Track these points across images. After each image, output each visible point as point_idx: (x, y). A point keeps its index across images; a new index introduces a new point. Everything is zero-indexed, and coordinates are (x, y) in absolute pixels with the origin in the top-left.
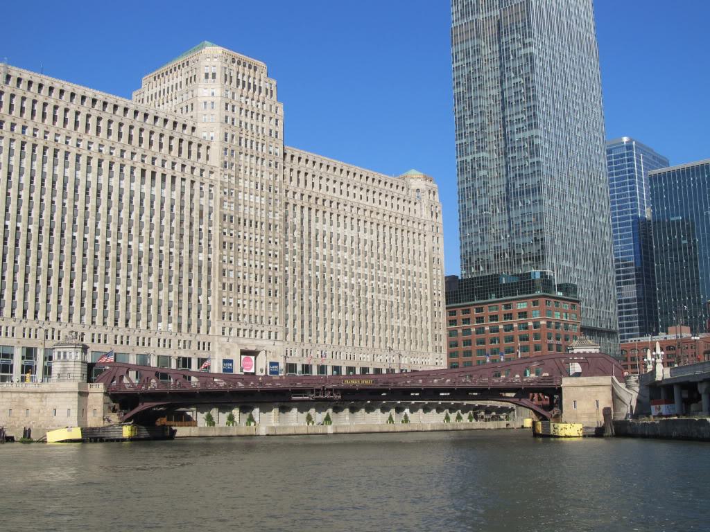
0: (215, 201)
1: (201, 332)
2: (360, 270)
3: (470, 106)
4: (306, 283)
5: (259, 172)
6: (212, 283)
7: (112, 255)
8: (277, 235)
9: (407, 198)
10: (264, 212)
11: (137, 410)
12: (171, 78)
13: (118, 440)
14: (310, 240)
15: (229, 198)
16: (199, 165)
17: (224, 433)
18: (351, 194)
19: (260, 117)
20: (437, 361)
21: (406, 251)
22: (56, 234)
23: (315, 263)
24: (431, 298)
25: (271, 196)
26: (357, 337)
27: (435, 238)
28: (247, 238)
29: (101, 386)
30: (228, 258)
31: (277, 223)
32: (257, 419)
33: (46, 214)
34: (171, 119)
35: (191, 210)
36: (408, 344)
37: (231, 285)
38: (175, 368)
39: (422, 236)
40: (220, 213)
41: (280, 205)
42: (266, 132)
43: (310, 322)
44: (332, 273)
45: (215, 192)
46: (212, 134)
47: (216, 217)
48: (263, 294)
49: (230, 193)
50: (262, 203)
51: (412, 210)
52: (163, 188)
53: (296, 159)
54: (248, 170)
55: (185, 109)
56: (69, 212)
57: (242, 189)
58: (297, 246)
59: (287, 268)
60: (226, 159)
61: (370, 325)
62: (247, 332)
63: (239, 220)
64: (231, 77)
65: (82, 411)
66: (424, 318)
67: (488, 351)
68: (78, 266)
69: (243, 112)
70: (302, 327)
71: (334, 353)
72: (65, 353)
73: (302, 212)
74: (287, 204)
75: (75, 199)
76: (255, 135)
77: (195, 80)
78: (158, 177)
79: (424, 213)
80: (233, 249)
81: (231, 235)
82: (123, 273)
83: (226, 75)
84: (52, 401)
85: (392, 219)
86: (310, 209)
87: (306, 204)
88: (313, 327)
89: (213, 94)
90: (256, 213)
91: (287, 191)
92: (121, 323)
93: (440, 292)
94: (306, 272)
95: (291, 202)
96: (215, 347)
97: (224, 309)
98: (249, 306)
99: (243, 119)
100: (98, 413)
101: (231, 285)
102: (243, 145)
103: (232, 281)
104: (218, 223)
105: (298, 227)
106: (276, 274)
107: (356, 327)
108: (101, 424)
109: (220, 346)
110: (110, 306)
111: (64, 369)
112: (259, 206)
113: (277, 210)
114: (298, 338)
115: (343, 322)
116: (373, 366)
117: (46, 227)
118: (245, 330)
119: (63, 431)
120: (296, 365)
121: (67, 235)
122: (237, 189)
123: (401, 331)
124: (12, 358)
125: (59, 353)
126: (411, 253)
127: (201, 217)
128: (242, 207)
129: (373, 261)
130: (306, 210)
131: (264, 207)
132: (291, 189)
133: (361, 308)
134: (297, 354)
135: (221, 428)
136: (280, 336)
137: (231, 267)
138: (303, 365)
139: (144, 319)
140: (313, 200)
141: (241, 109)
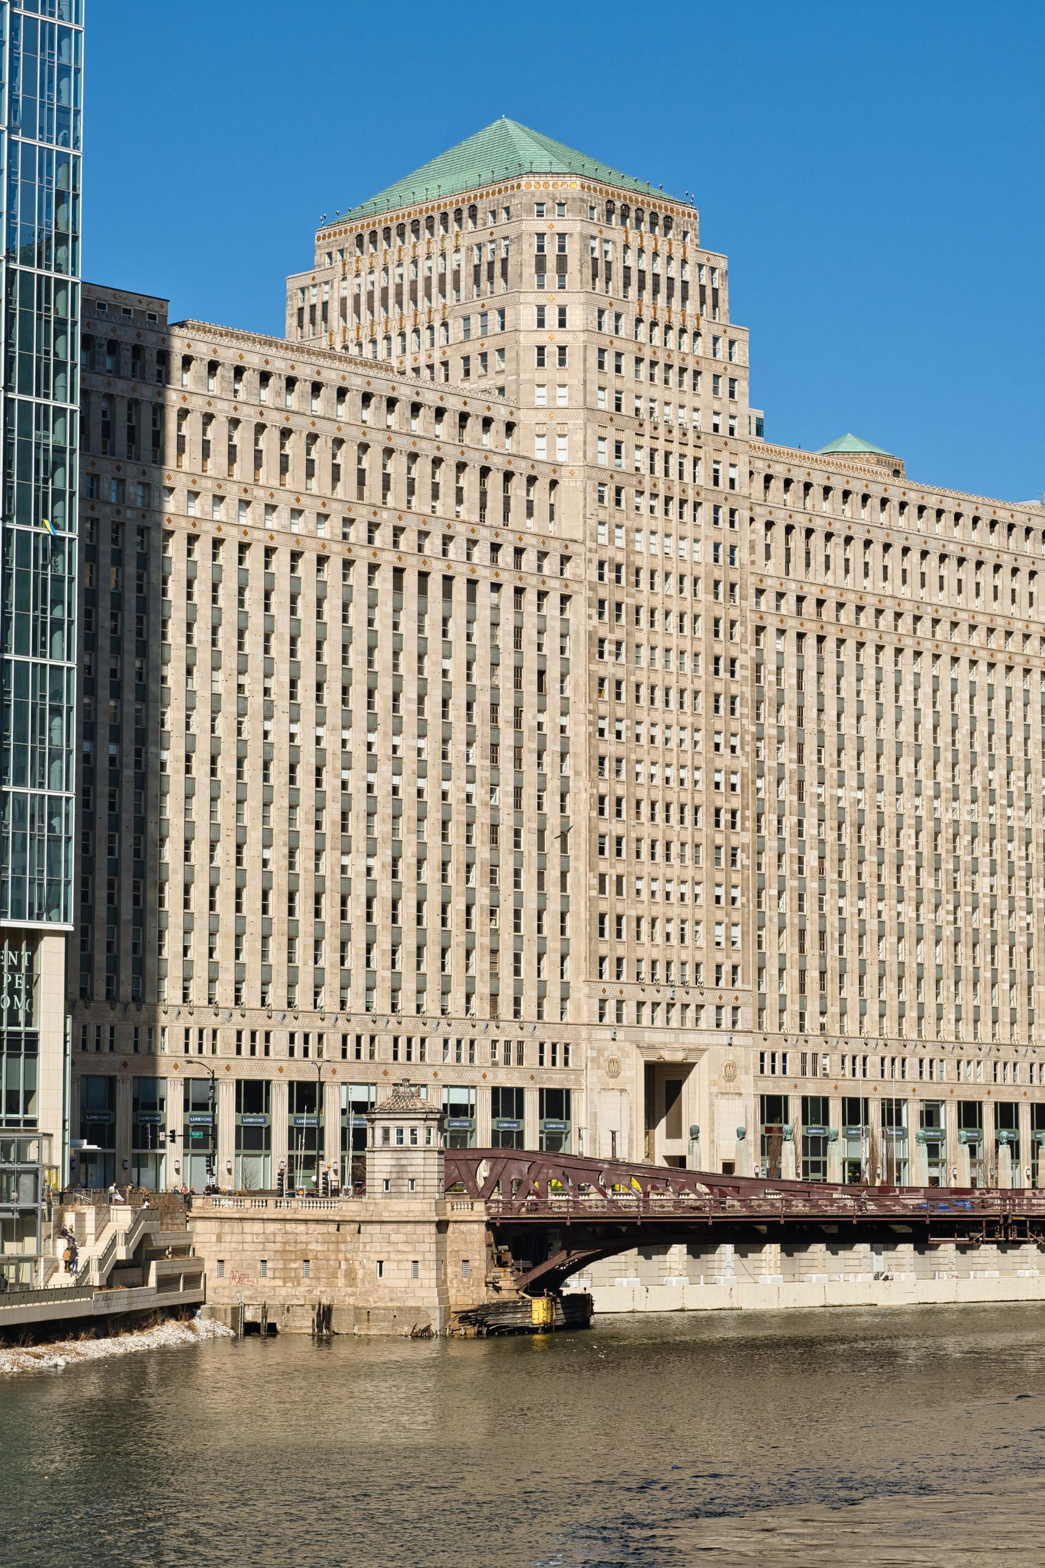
1: (546, 1018)
4: (811, 860)
19: (688, 377)
41: (743, 637)
43: (822, 974)
58: (787, 754)
71: (887, 1062)
72: (400, 1132)
73: (799, 649)
77: (504, 274)
80: (623, 777)
81: (619, 734)
86: (821, 639)
107: (948, 983)
108: (483, 1296)
109: (594, 1054)
116: (993, 1099)
120: (786, 1097)
125: (386, 1131)
130: (810, 641)
133: (960, 924)
136: (746, 1017)
138: (805, 1099)
141: (639, 360)
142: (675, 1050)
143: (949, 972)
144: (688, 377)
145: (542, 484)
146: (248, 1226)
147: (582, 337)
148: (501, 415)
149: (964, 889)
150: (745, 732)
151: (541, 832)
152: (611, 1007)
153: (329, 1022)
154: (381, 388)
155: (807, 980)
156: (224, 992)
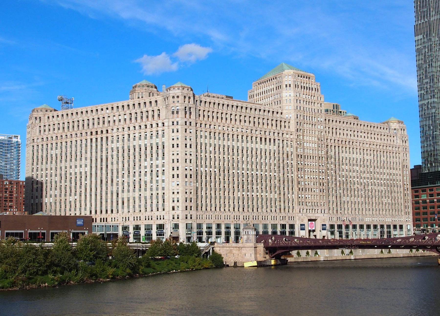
0: (294, 149)
1: (290, 212)
2: (365, 175)
3: (426, 71)
4: (338, 184)
5: (313, 132)
6: (293, 188)
7: (250, 179)
8: (323, 162)
9: (389, 135)
10: (317, 151)
11: (276, 253)
12: (268, 85)
13: (270, 266)
14: (339, 163)
15: (300, 146)
16: (285, 132)
17: (305, 260)
18: (359, 136)
19: (313, 103)
20: (407, 219)
21: (389, 163)
22: (226, 172)
23: (342, 174)
24: (403, 187)
25: (320, 143)
26: (364, 210)
27: (405, 154)
28: (309, 165)
29: (262, 244)
30: (301, 176)
31: (323, 156)
32: (319, 253)
33: (221, 163)
34: (271, 110)
35: (283, 154)
36: (391, 211)
37: (303, 189)
38: (288, 235)
39: (398, 154)
40: (296, 154)
41: (324, 147)
42: (316, 111)
43: (341, 203)
44: (351, 178)
45: (294, 144)
46: (290, 116)
47: (294, 156)
48: (318, 191)
49: (300, 144)
50: (316, 146)
51: (392, 141)
52: (270, 145)
53: (331, 121)
54: (308, 131)
55: (276, 103)
56: (231, 161)
57: (306, 141)
58: (333, 166)
59: (328, 178)
60: (298, 127)
61: (371, 203)
62: (311, 211)
63: (305, 156)
64: (298, 85)
65: (256, 253)
66: (400, 197)
67: (436, 212)
68: (236, 186)
69: (305, 102)
70: (337, 206)
72: (248, 232)
73: (335, 148)
74: (327, 146)
75: (233, 155)
76: (311, 113)
77: (280, 88)
78: (268, 140)
79: (398, 141)
80: (303, 171)
81: (302, 164)
82: (255, 187)
83: (296, 85)
84: (244, 251)
85: (381, 147)
86: (339, 147)
87: (337, 145)
88: (342, 206)
89: (290, 95)
90: (313, 152)
91: (327, 139)
92: (255, 210)
93: (408, 183)
94: (338, 179)
95: (330, 145)
96: (296, 218)
97: (300, 200)
98: (311, 198)
99: (305, 106)
100: (262, 256)
101: (303, 189)
102: (305, 119)
103: (303, 187)
104: (295, 159)
105: (333, 156)
106: (324, 181)
107: (364, 205)
108: (263, 259)
110: (250, 203)
111: (248, 238)
112: (314, 148)
113: (323, 149)
114: (335, 212)
115: (357, 203)
117: (222, 169)
118: (310, 209)
119: (249, 263)
121: (231, 172)
122: (303, 141)
123: (387, 205)
124: (212, 229)
125: (246, 232)
126: (392, 164)
127: (288, 157)
128: (306, 150)
129: (372, 170)
130: (337, 147)
131: (317, 149)
132: (329, 138)
133: (366, 194)
134: (335, 219)
135: (304, 258)
136: (326, 211)
137: (302, 180)
138: (338, 225)
139: (265, 207)
140: (340, 142)
141: (304, 101)
142: (313, 217)
143: (364, 202)
144: (313, 103)
145: (287, 122)
146: (224, 248)
147: (293, 98)
148: (280, 111)
149: (366, 188)
150: (325, 163)
151: (288, 181)
152: (301, 210)
153: (250, 214)
154: (258, 107)
155: (338, 205)
156: (231, 209)
